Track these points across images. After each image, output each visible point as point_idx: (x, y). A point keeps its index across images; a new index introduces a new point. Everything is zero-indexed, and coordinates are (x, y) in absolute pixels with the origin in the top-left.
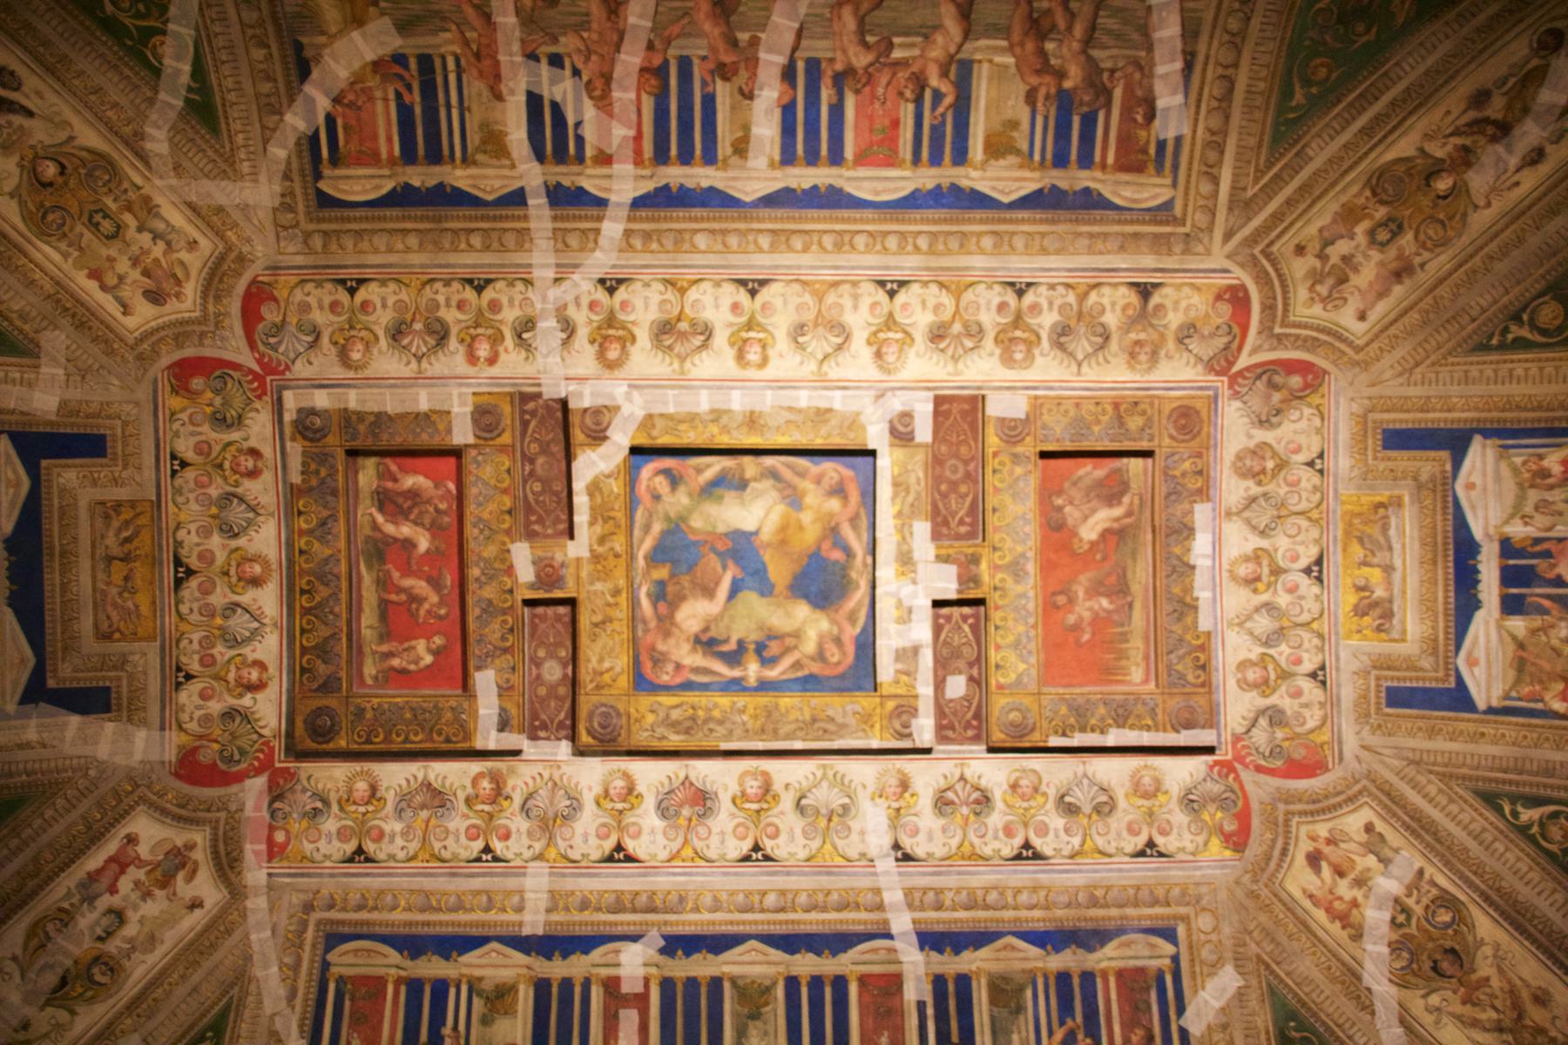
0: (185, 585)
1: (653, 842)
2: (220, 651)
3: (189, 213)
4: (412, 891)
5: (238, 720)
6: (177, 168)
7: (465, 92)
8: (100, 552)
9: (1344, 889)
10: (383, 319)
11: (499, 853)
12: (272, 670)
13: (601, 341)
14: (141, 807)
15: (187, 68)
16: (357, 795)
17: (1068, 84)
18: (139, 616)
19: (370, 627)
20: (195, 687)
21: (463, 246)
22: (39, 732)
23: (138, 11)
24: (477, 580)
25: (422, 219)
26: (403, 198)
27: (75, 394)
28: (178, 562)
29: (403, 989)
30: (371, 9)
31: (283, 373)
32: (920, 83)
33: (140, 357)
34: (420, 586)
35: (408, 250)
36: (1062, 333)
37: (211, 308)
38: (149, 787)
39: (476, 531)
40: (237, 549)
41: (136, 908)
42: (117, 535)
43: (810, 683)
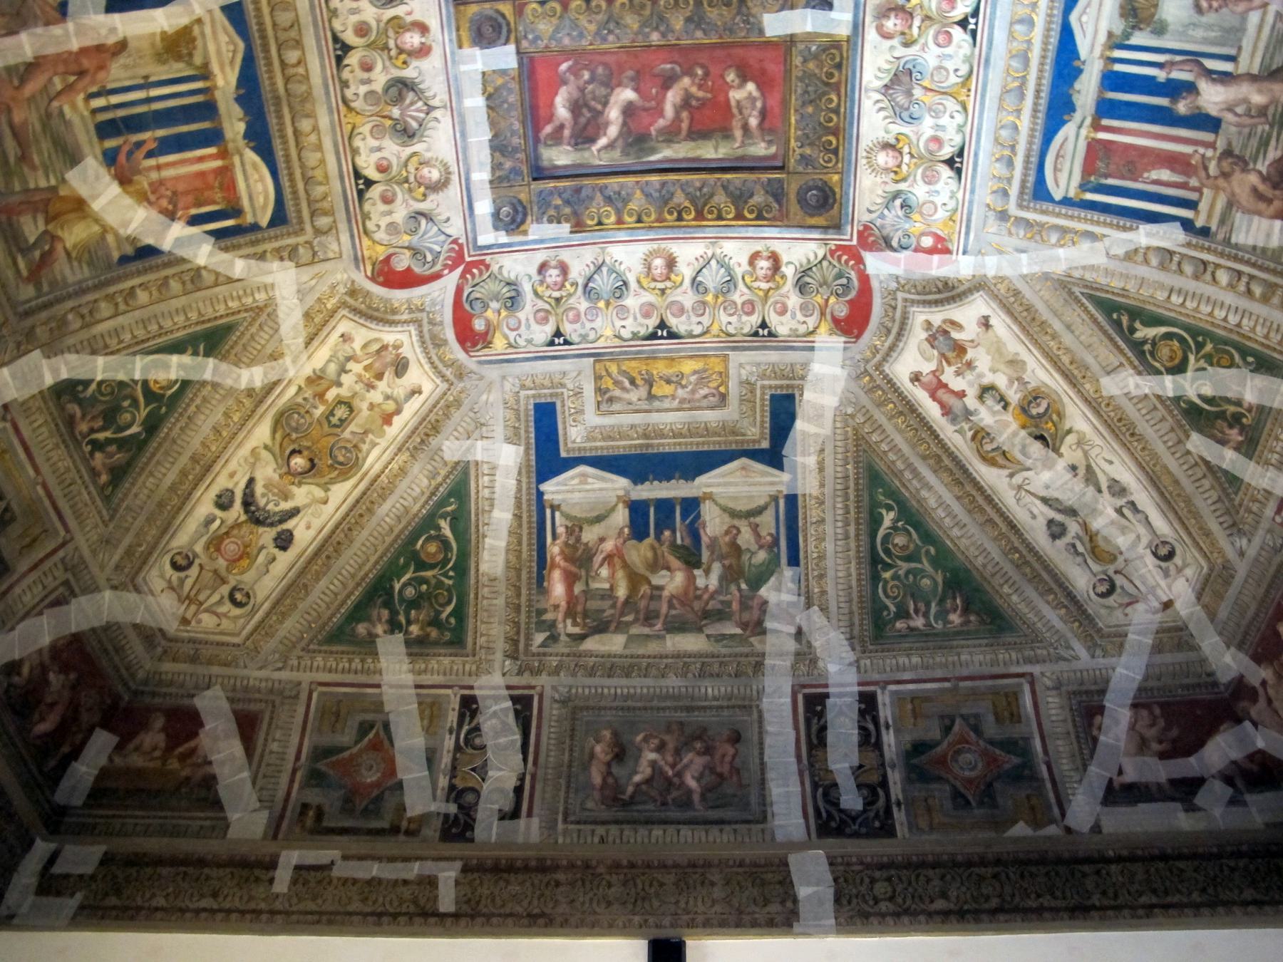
0: (675, 329)
3: (315, 343)
6: (275, 356)
7: (127, 83)
10: (392, 150)
11: (969, 10)
12: (758, 246)
14: (886, 368)
15: (175, 359)
16: (891, 163)
18: (705, 371)
19: (716, 149)
20: (774, 320)
21: (301, 70)
23: (130, 406)
24: (664, 35)
25: (280, 117)
26: (260, 139)
27: (499, 431)
28: (653, 336)
29: (1105, 122)
30: (62, 192)
31: (461, 246)
33: (460, 376)
34: (672, 97)
35: (315, 128)
37: (405, 317)
38: (867, 361)
39: (611, 38)
40: (639, 282)
41: (981, 376)
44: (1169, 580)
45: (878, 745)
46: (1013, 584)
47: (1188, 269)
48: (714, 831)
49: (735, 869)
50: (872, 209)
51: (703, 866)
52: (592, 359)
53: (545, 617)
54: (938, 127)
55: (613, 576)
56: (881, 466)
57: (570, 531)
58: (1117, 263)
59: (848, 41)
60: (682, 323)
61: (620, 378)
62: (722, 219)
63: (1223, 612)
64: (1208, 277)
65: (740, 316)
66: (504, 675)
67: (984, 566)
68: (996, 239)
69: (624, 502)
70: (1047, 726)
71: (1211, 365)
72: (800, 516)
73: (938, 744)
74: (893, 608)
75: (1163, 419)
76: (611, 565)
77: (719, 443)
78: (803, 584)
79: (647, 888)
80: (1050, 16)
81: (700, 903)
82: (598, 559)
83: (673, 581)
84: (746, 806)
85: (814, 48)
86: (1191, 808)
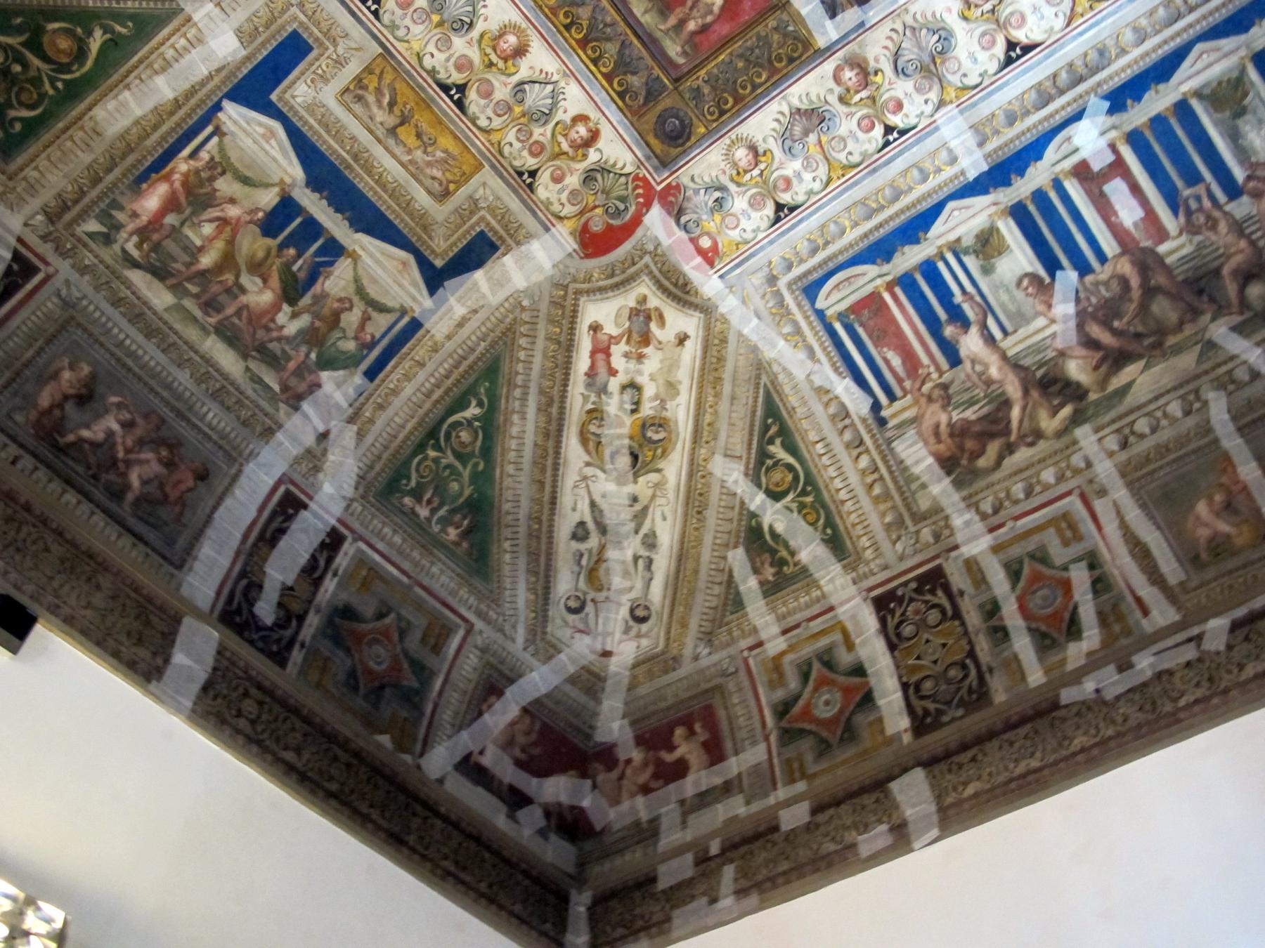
0: (467, 102)
1: (1042, 17)
2: (541, 133)
4: (848, 209)
5: (599, 176)
8: (380, 132)
11: (901, 126)
12: (593, 114)
14: (583, 299)
16: (743, 164)
19: (646, 12)
20: (544, 178)
22: (463, 305)
27: (240, 16)
28: (445, 88)
29: (898, 290)
38: (575, 280)
40: (482, 36)
41: (639, 372)
42: (380, 106)
44: (625, 637)
45: (317, 583)
46: (516, 545)
47: (848, 436)
48: (127, 541)
49: (129, 591)
50: (696, 179)
51: (99, 564)
52: (380, 50)
53: (114, 213)
54: (798, 175)
55: (211, 239)
56: (505, 367)
57: (212, 164)
58: (808, 387)
59: (815, 51)
60: (478, 105)
61: (386, 92)
62: (596, 65)
63: (642, 690)
64: (855, 453)
65: (524, 148)
66: (26, 225)
67: (508, 513)
68: (750, 290)
69: (283, 190)
70: (454, 675)
71: (799, 512)
72: (409, 345)
73: (365, 622)
74: (413, 483)
75: (731, 520)
76: (219, 230)
77: (406, 224)
78: (362, 399)
79: (29, 541)
80: (940, 188)
81: (74, 596)
82: (214, 213)
83: (259, 295)
84: (171, 542)
85: (791, 28)
86: (511, 816)
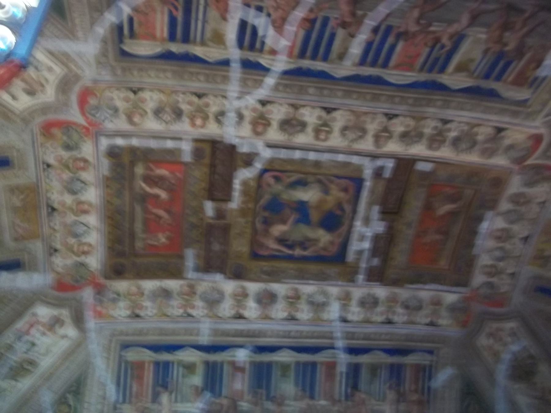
9: (497, 347)
13: (255, 123)
17: (507, 48)
26: (168, 56)
32: (437, 40)
34: (161, 213)
36: (456, 142)
43: (319, 259)
